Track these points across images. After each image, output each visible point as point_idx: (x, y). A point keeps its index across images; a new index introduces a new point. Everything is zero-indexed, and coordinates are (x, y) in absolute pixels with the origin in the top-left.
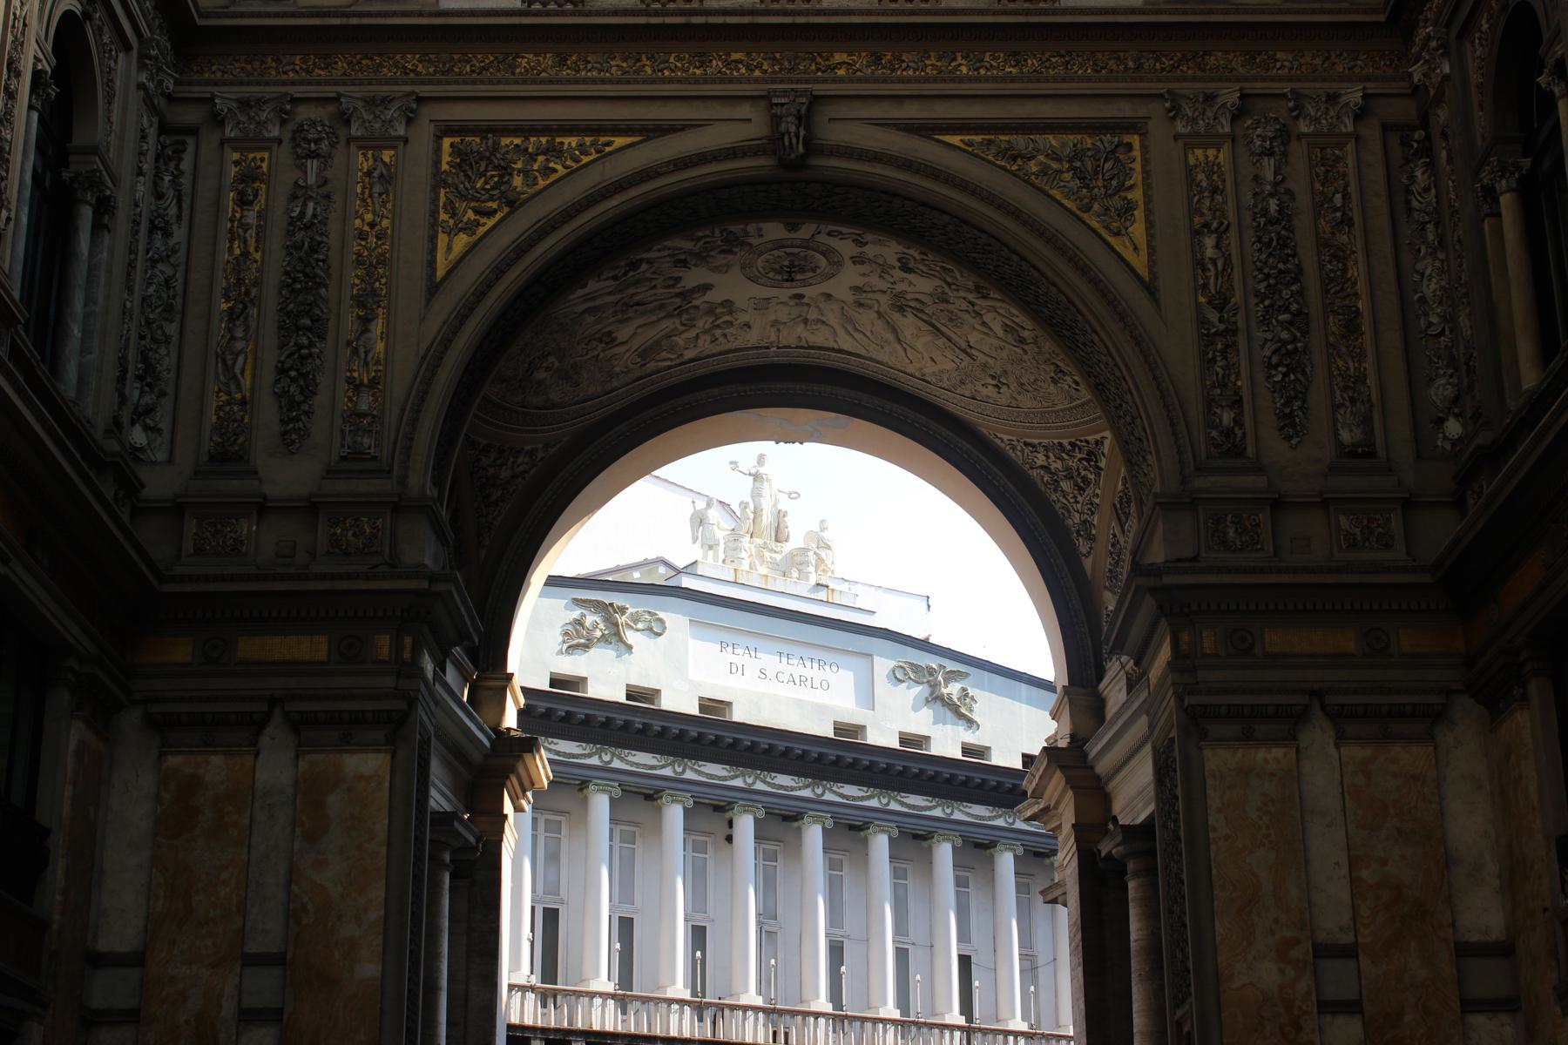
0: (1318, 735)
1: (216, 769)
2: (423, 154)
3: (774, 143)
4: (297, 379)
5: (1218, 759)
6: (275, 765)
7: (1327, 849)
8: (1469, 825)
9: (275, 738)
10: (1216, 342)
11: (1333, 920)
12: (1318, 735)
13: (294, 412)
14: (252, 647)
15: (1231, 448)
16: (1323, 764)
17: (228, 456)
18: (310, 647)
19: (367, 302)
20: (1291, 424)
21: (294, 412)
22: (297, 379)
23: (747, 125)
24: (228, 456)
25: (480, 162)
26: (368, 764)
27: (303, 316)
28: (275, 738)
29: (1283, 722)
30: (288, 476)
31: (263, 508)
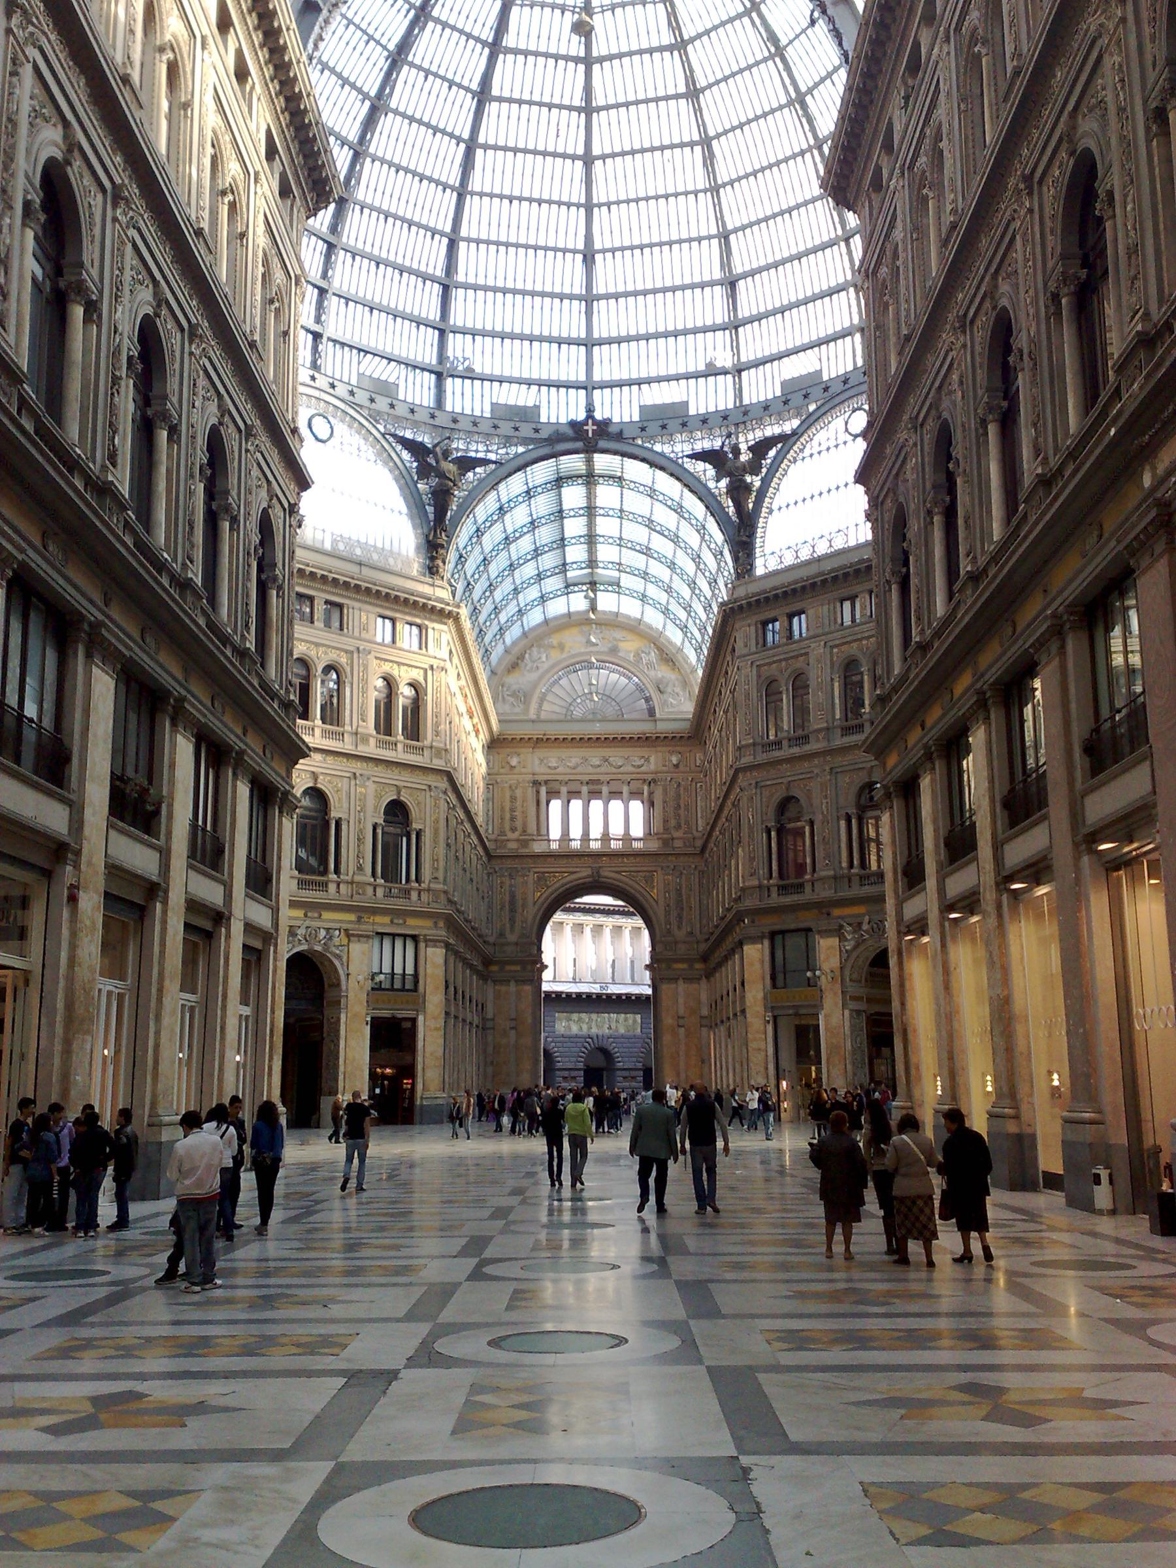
0: (681, 982)
1: (503, 988)
2: (532, 878)
3: (592, 876)
4: (512, 921)
5: (664, 987)
6: (513, 987)
7: (681, 1001)
8: (704, 997)
9: (512, 984)
10: (668, 913)
11: (681, 1012)
12: (681, 982)
13: (512, 927)
14: (508, 968)
15: (669, 931)
16: (682, 986)
17: (502, 935)
18: (518, 968)
19: (524, 906)
20: (679, 928)
21: (512, 927)
22: (512, 921)
23: (588, 872)
24: (502, 935)
25: (541, 879)
26: (528, 988)
27: (513, 910)
28: (512, 984)
29: (676, 980)
30: (512, 938)
31: (508, 944)
